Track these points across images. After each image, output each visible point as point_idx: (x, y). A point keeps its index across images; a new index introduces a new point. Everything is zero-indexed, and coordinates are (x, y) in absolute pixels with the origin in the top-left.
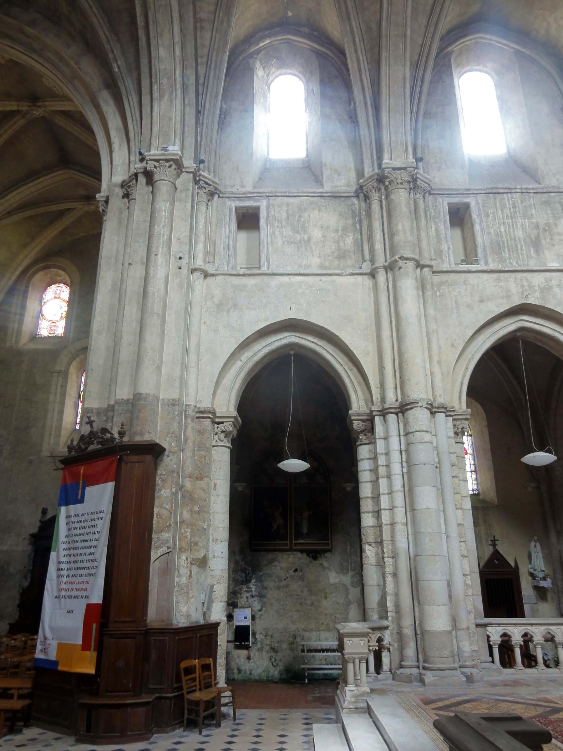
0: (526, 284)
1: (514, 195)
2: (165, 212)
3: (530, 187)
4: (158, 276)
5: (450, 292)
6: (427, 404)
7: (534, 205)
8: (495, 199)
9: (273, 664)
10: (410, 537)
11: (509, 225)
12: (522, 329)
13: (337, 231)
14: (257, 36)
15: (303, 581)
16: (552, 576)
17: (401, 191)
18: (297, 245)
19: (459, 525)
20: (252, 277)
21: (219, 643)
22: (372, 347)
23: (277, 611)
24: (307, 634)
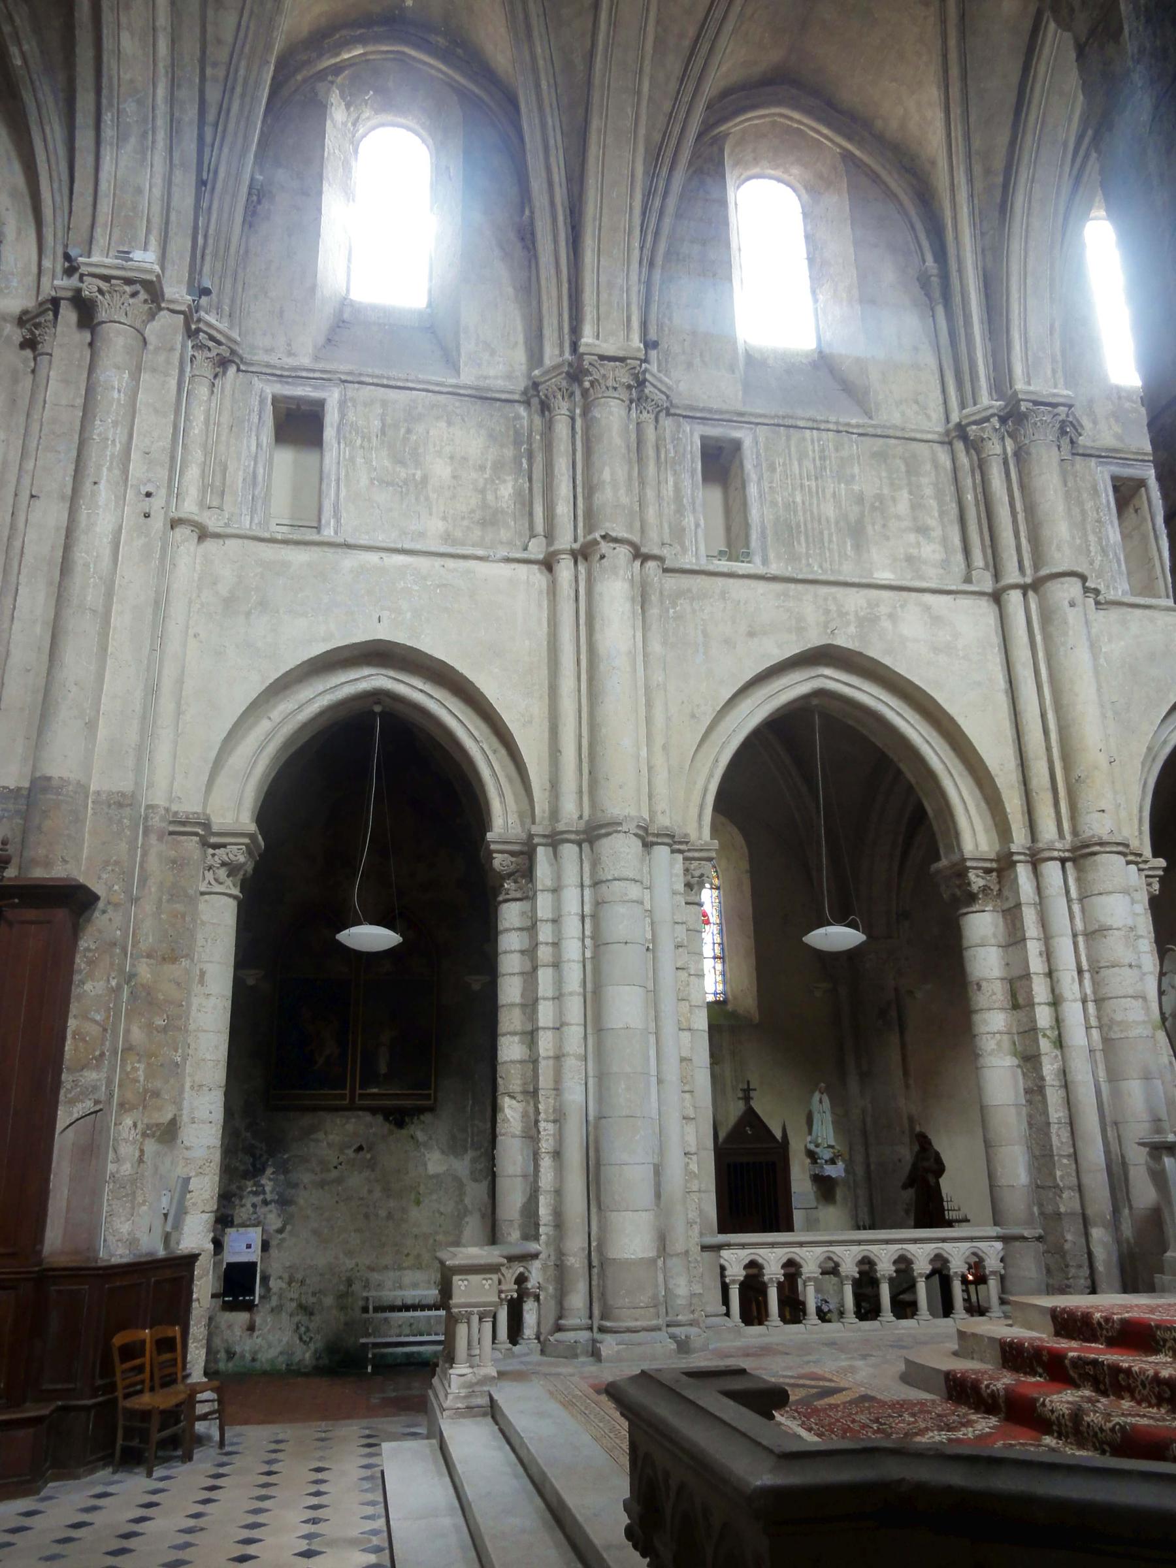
0: (833, 608)
1: (824, 435)
2: (119, 391)
3: (854, 421)
4: (98, 529)
5: (694, 611)
6: (639, 827)
7: (859, 457)
8: (788, 438)
9: (301, 1339)
10: (591, 1082)
12: (820, 693)
13: (482, 468)
14: (337, 36)
15: (373, 1170)
16: (847, 1157)
17: (614, 403)
18: (400, 489)
19: (683, 1060)
20: (302, 547)
21: (195, 1296)
22: (538, 709)
23: (315, 1232)
24: (375, 1277)
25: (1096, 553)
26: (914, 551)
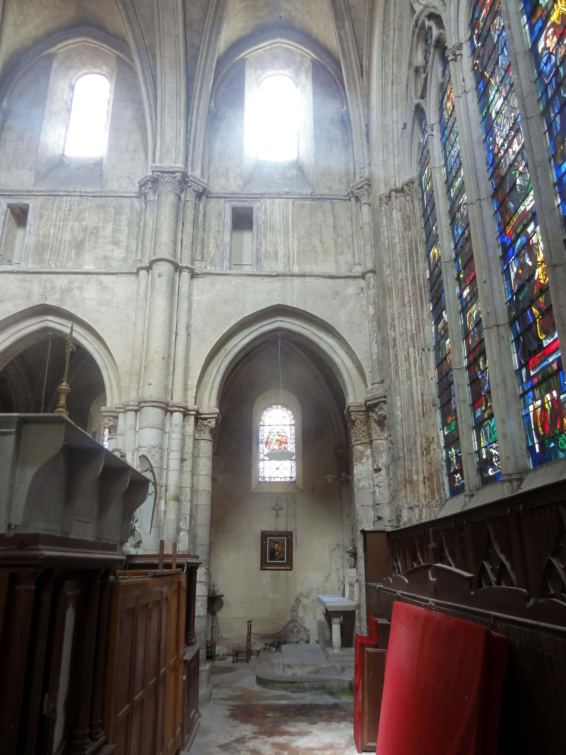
0: (49, 285)
1: (74, 198)
3: (89, 190)
7: (90, 208)
8: (54, 202)
11: (59, 227)
25: (213, 248)
26: (109, 254)
